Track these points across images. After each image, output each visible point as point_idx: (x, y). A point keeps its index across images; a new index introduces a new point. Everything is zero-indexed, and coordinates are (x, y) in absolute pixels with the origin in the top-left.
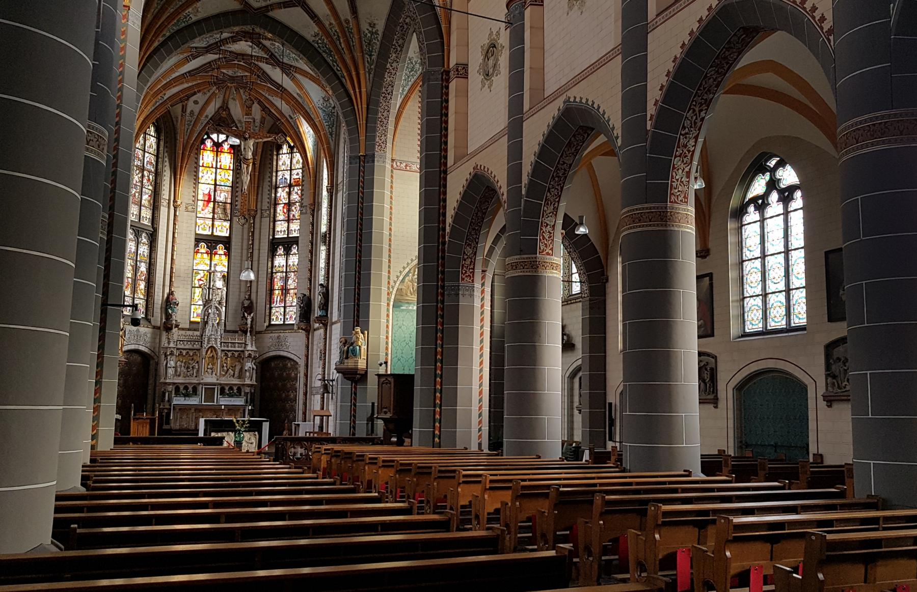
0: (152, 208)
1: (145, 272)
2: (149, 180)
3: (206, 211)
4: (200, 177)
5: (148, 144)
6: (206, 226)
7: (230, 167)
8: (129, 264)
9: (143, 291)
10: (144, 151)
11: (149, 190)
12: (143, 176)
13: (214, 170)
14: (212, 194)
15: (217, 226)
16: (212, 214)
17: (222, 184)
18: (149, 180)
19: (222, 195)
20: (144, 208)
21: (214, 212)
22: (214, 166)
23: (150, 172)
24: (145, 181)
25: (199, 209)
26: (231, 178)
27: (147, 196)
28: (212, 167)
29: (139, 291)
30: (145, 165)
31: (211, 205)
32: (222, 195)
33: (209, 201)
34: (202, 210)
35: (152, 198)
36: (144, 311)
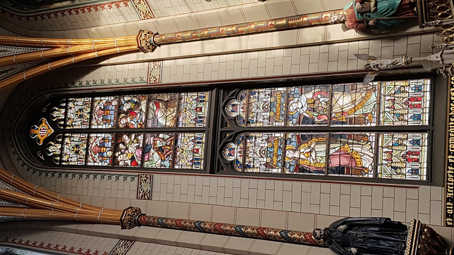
0: (177, 95)
1: (310, 96)
2: (130, 112)
5: (78, 125)
8: (296, 155)
9: (359, 97)
10: (90, 131)
11: (148, 108)
12: (128, 131)
18: (130, 112)
20: (181, 119)
23: (119, 111)
24: (134, 123)
27: (159, 114)
29: (359, 112)
30: (110, 126)
35: (160, 97)
36: (413, 83)
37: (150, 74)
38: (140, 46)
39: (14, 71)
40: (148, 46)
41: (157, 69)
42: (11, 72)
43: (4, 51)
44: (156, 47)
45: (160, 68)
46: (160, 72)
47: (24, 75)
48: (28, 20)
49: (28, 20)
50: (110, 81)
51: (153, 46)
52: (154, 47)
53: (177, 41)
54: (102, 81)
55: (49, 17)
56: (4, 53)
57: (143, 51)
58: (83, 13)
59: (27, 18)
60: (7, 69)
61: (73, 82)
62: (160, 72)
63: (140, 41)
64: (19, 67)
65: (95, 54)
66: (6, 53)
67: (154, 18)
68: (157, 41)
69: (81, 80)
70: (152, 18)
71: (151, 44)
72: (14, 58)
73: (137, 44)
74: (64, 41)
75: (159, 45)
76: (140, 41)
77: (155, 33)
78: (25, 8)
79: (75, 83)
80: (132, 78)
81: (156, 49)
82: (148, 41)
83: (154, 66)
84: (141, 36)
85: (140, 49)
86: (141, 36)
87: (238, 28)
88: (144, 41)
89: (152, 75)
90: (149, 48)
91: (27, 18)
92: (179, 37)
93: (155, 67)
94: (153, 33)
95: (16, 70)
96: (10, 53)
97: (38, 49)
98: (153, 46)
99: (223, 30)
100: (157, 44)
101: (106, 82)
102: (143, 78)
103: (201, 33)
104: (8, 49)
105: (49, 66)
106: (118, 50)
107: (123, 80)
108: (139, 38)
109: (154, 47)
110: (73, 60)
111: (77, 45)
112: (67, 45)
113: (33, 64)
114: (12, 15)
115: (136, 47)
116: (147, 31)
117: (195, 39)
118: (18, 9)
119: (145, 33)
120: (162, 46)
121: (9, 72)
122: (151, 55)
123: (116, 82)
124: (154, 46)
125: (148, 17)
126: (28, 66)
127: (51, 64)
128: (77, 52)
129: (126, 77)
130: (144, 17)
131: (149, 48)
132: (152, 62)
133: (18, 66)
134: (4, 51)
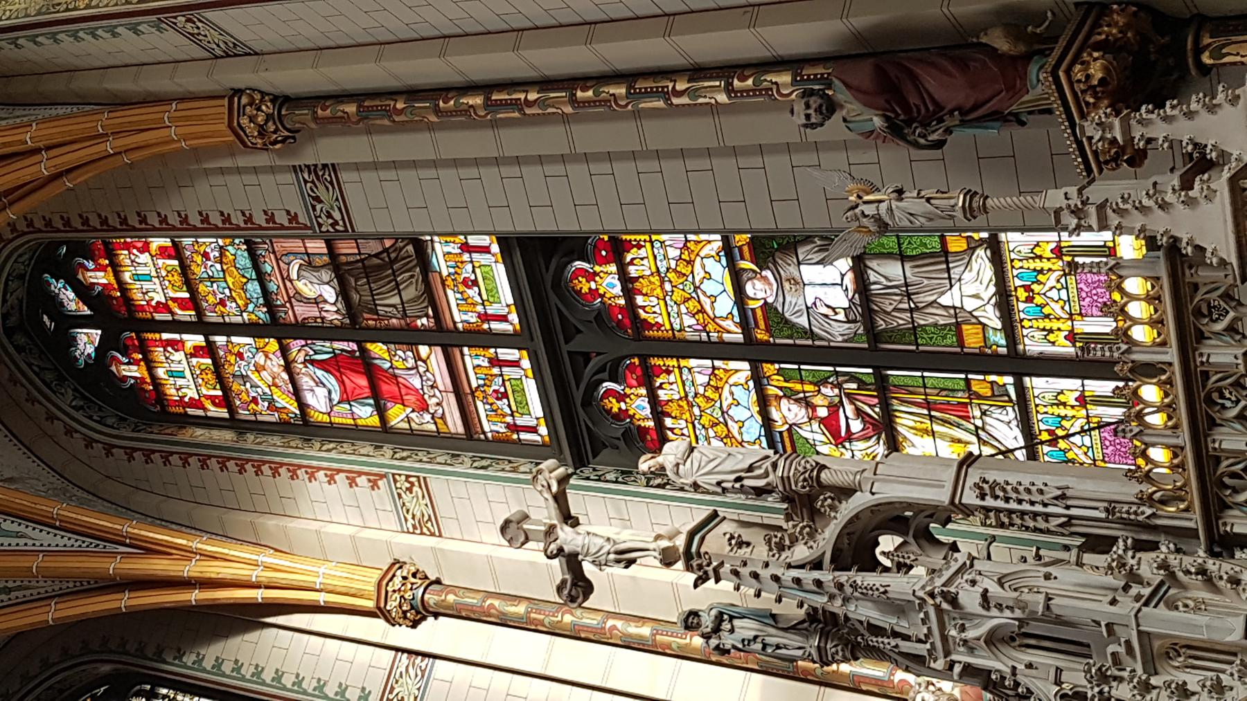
3: (416, 382)
4: (274, 418)
6: (497, 385)
7: (163, 252)
13: (220, 340)
14: (325, 349)
15: (472, 318)
16: (424, 350)
17: (254, 288)
19: (308, 288)
21: (407, 337)
22: (199, 340)
25: (424, 422)
26: (209, 244)
28: (209, 350)
31: (377, 349)
32: (308, 288)
33: (367, 365)
34: (424, 407)
37: (392, 689)
38: (382, 605)
39: (28, 593)
40: (405, 612)
41: (413, 675)
42: (20, 594)
43: (19, 535)
44: (424, 618)
45: (423, 676)
46: (419, 689)
47: (53, 613)
48: (109, 453)
49: (109, 453)
50: (278, 676)
51: (418, 612)
52: (419, 616)
53: (485, 619)
54: (258, 671)
55: (166, 461)
56: (14, 541)
57: (388, 620)
58: (257, 475)
59: (109, 449)
60: (10, 584)
61: (179, 650)
62: (419, 689)
63: (387, 592)
64: (47, 586)
65: (258, 595)
66: (22, 541)
67: (440, 536)
68: (431, 602)
69: (202, 652)
70: (432, 534)
71: (412, 607)
72: (35, 563)
73: (375, 598)
74: (184, 542)
75: (436, 615)
76: (387, 592)
77: (433, 578)
78: (110, 421)
79: (184, 653)
80: (341, 684)
81: (424, 623)
82: (406, 596)
83: (407, 667)
84: (391, 579)
85: (379, 612)
86: (391, 579)
87: (657, 634)
88: (397, 595)
89: (395, 692)
90: (405, 618)
91: (109, 449)
92: (493, 611)
93: (410, 668)
94: (426, 578)
95: (35, 592)
96: (30, 542)
97: (111, 547)
98: (418, 612)
99: (614, 627)
100: (431, 609)
101: (268, 676)
102: (370, 692)
103: (553, 616)
104: (29, 531)
105: (126, 601)
106: (322, 598)
107: (314, 684)
108: (384, 583)
109: (419, 616)
110: (195, 596)
111: (216, 558)
112: (188, 554)
113: (85, 583)
114: (69, 432)
115: (370, 604)
116: (413, 569)
117: (533, 627)
118: (90, 418)
119: (405, 574)
120: (441, 618)
121: (13, 595)
122: (403, 636)
123: (294, 684)
124: (417, 614)
125: (425, 530)
126: (68, 587)
127: (133, 595)
128: (210, 578)
129: (324, 678)
130: (414, 527)
131: (405, 618)
132: (405, 655)
133: (42, 584)
134: (19, 535)
